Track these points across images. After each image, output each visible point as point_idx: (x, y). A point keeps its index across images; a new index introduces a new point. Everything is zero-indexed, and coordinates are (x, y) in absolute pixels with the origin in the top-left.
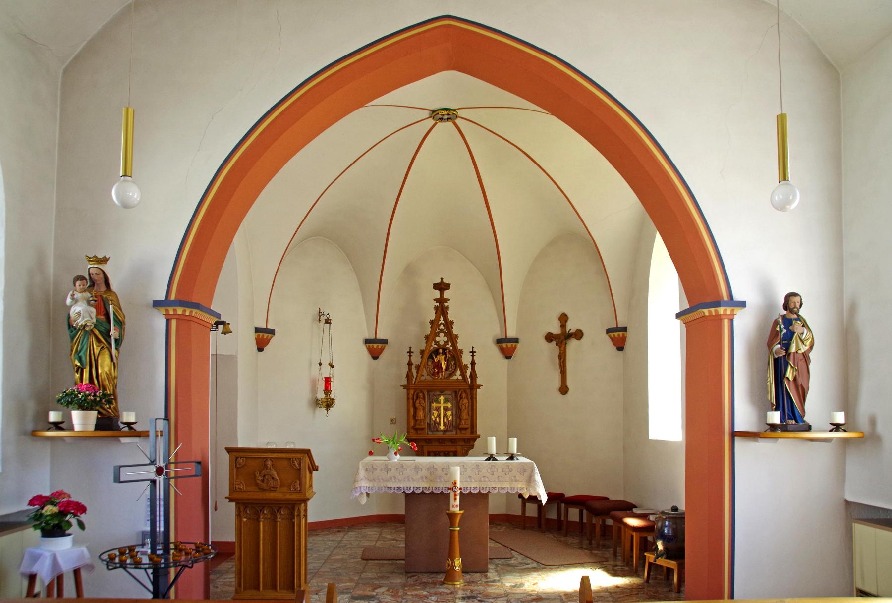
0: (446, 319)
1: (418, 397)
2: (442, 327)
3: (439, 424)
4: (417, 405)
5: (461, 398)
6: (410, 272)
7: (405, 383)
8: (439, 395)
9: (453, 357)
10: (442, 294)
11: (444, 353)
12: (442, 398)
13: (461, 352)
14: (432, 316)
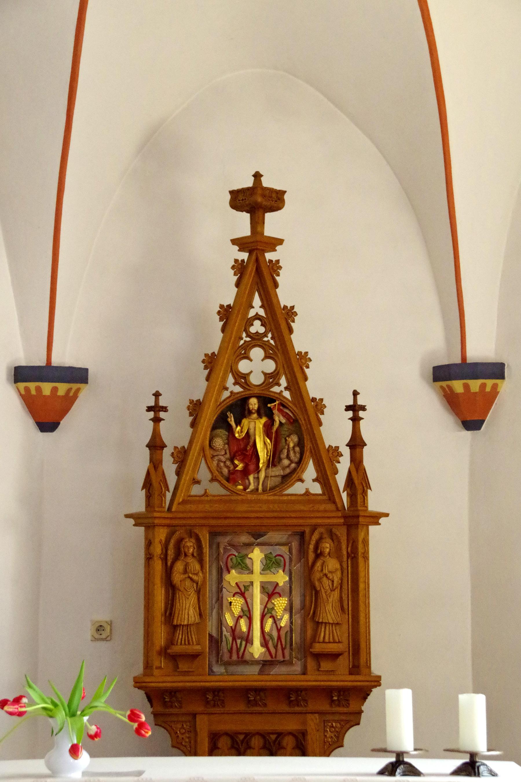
0: (269, 302)
2: (257, 327)
3: (248, 639)
5: (318, 555)
7: (139, 505)
8: (249, 546)
9: (294, 421)
10: (257, 223)
11: (265, 411)
12: (257, 556)
13: (319, 406)
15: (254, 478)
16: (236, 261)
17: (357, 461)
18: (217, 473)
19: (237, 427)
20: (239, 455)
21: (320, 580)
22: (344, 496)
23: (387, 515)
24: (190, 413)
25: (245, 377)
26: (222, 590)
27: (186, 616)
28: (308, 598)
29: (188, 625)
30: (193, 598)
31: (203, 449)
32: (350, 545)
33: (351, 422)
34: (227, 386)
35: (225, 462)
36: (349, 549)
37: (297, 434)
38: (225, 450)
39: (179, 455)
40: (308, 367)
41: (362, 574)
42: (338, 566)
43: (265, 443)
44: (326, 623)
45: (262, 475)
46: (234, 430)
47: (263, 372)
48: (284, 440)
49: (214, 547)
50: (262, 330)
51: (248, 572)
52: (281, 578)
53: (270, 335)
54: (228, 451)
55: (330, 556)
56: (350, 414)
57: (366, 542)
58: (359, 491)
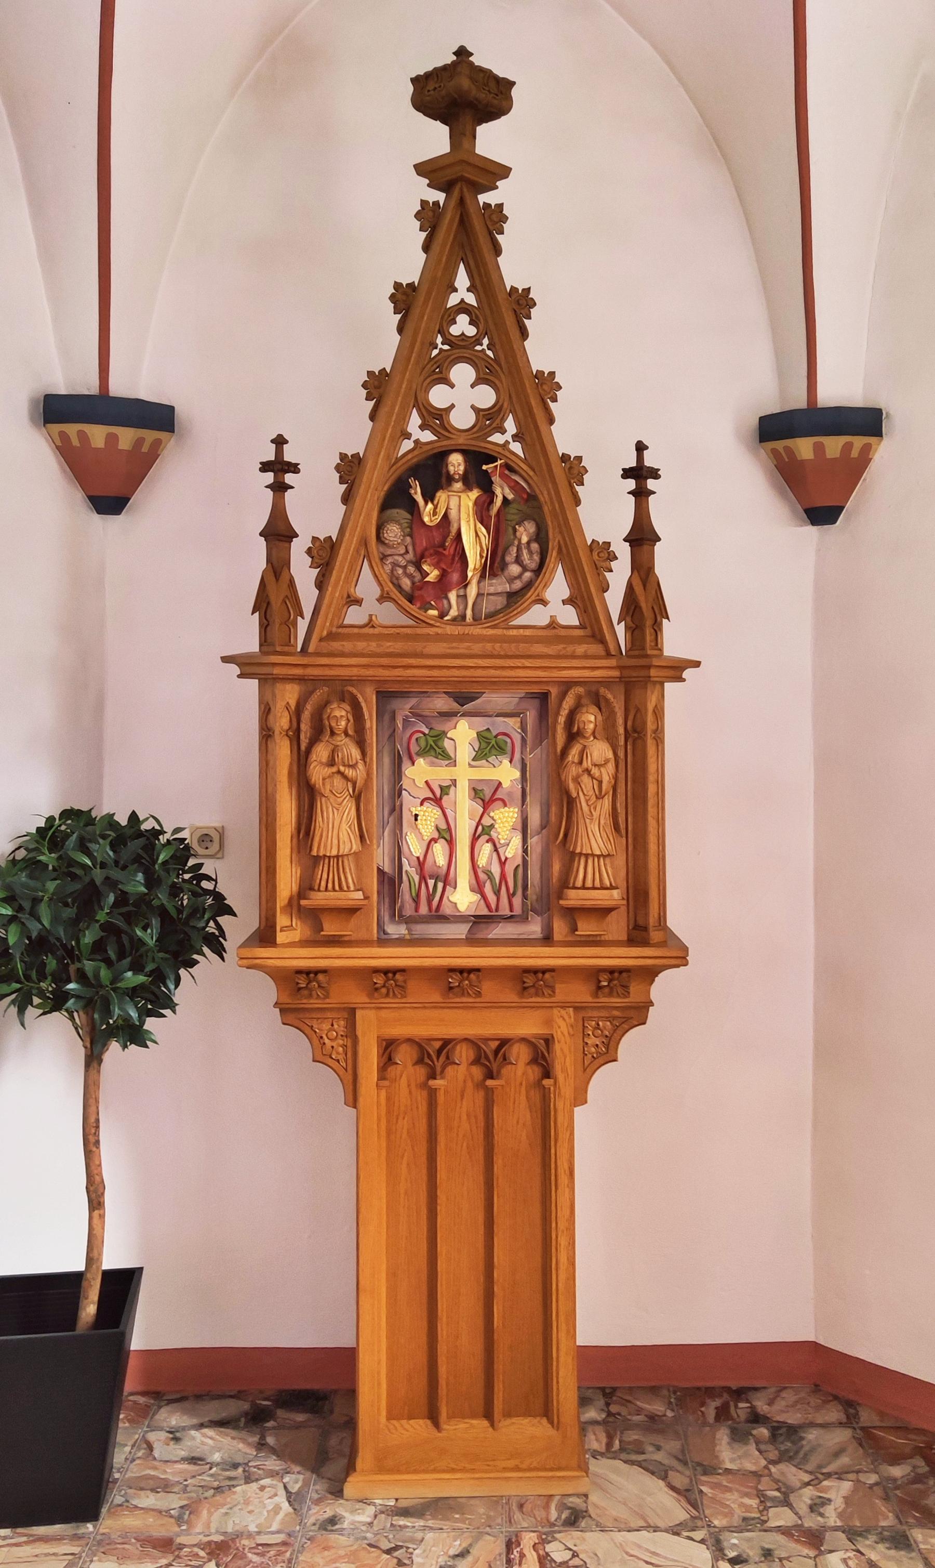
0: (485, 279)
1: (319, 730)
2: (462, 326)
3: (447, 879)
4: (317, 773)
7: (250, 644)
8: (449, 715)
10: (462, 137)
11: (477, 477)
12: (463, 735)
13: (574, 469)
14: (410, 265)
15: (458, 596)
16: (424, 203)
17: (643, 569)
18: (390, 585)
19: (426, 504)
20: (431, 555)
21: (576, 780)
22: (620, 630)
23: (697, 664)
24: (341, 477)
25: (441, 415)
26: (400, 794)
27: (335, 842)
28: (554, 809)
29: (337, 857)
30: (349, 808)
31: (364, 542)
32: (631, 717)
33: (632, 499)
34: (409, 430)
35: (405, 567)
36: (629, 723)
37: (534, 520)
38: (406, 547)
39: (321, 553)
40: (555, 400)
41: (652, 767)
42: (610, 755)
43: (477, 535)
44: (587, 856)
45: (472, 591)
46: (422, 509)
47: (473, 407)
48: (510, 530)
49: (387, 718)
50: (471, 331)
51: (447, 762)
52: (506, 773)
53: (486, 341)
54: (410, 549)
55: (595, 738)
56: (631, 484)
57: (659, 713)
58: (649, 623)
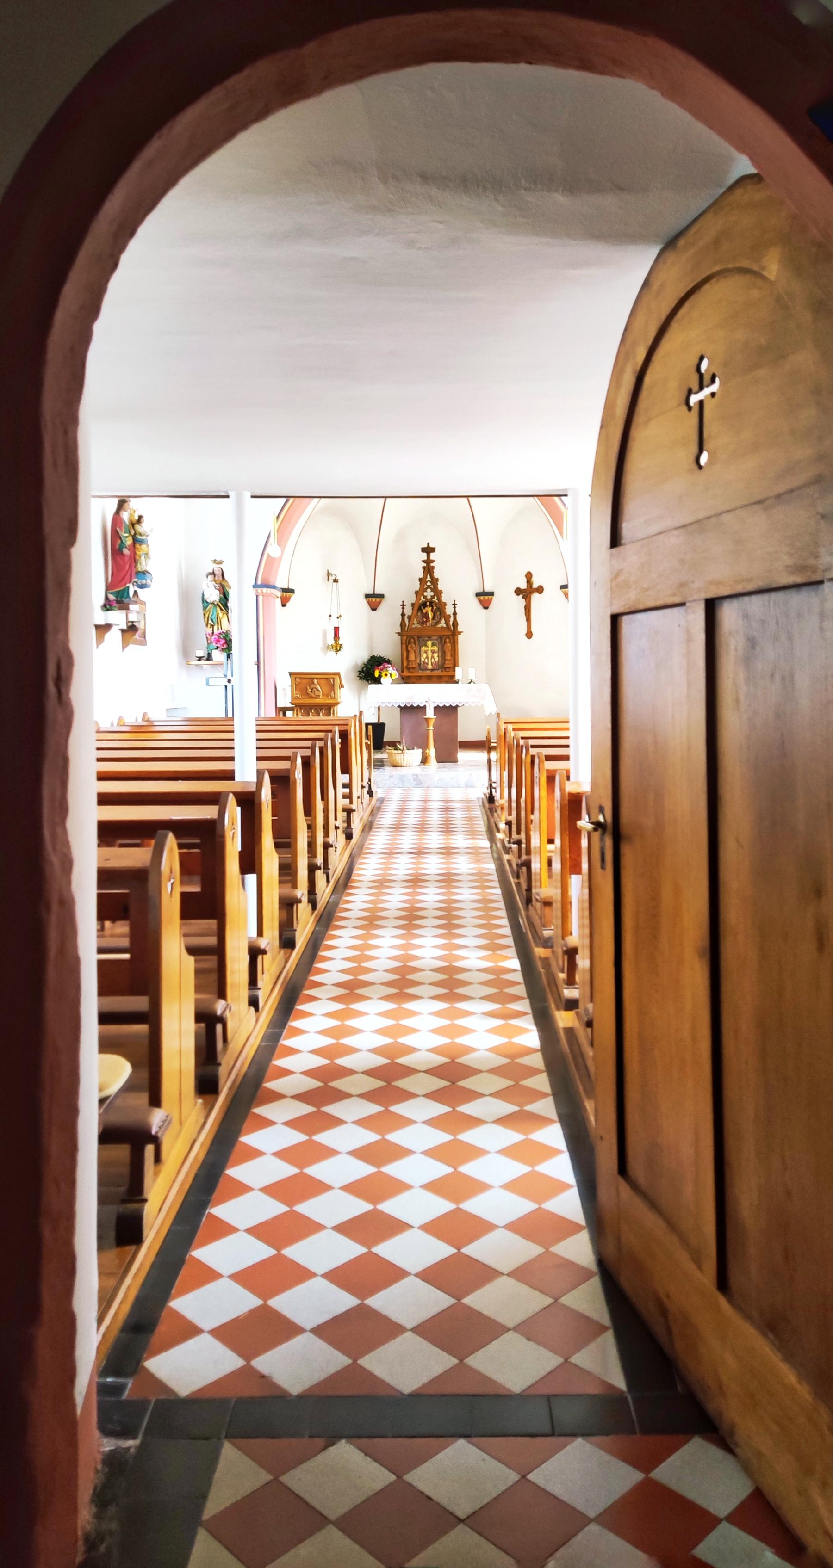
0: (432, 577)
1: (409, 642)
2: (429, 584)
3: (427, 664)
6: (401, 537)
7: (399, 631)
10: (428, 556)
11: (431, 605)
12: (429, 643)
13: (445, 604)
52: (436, 648)
